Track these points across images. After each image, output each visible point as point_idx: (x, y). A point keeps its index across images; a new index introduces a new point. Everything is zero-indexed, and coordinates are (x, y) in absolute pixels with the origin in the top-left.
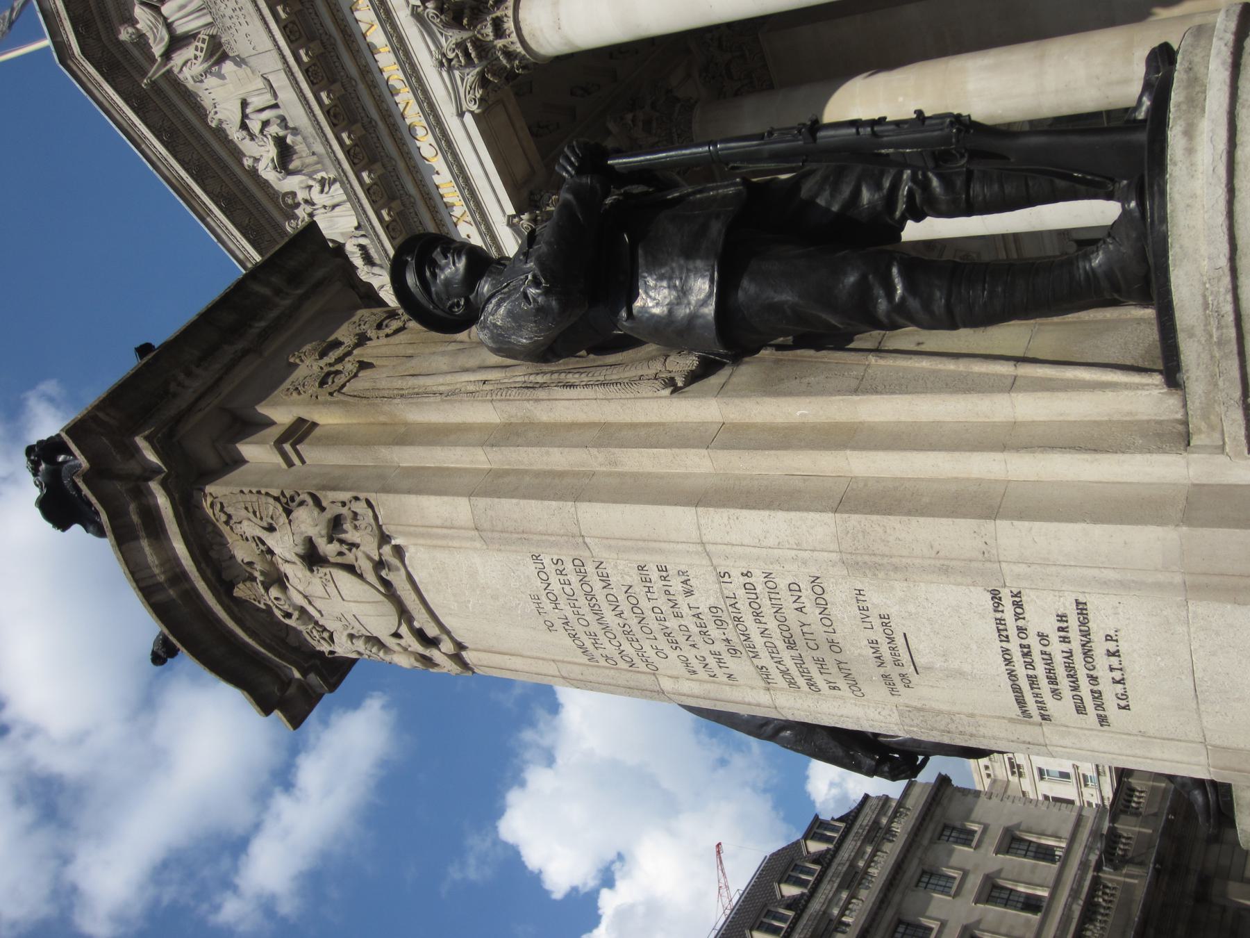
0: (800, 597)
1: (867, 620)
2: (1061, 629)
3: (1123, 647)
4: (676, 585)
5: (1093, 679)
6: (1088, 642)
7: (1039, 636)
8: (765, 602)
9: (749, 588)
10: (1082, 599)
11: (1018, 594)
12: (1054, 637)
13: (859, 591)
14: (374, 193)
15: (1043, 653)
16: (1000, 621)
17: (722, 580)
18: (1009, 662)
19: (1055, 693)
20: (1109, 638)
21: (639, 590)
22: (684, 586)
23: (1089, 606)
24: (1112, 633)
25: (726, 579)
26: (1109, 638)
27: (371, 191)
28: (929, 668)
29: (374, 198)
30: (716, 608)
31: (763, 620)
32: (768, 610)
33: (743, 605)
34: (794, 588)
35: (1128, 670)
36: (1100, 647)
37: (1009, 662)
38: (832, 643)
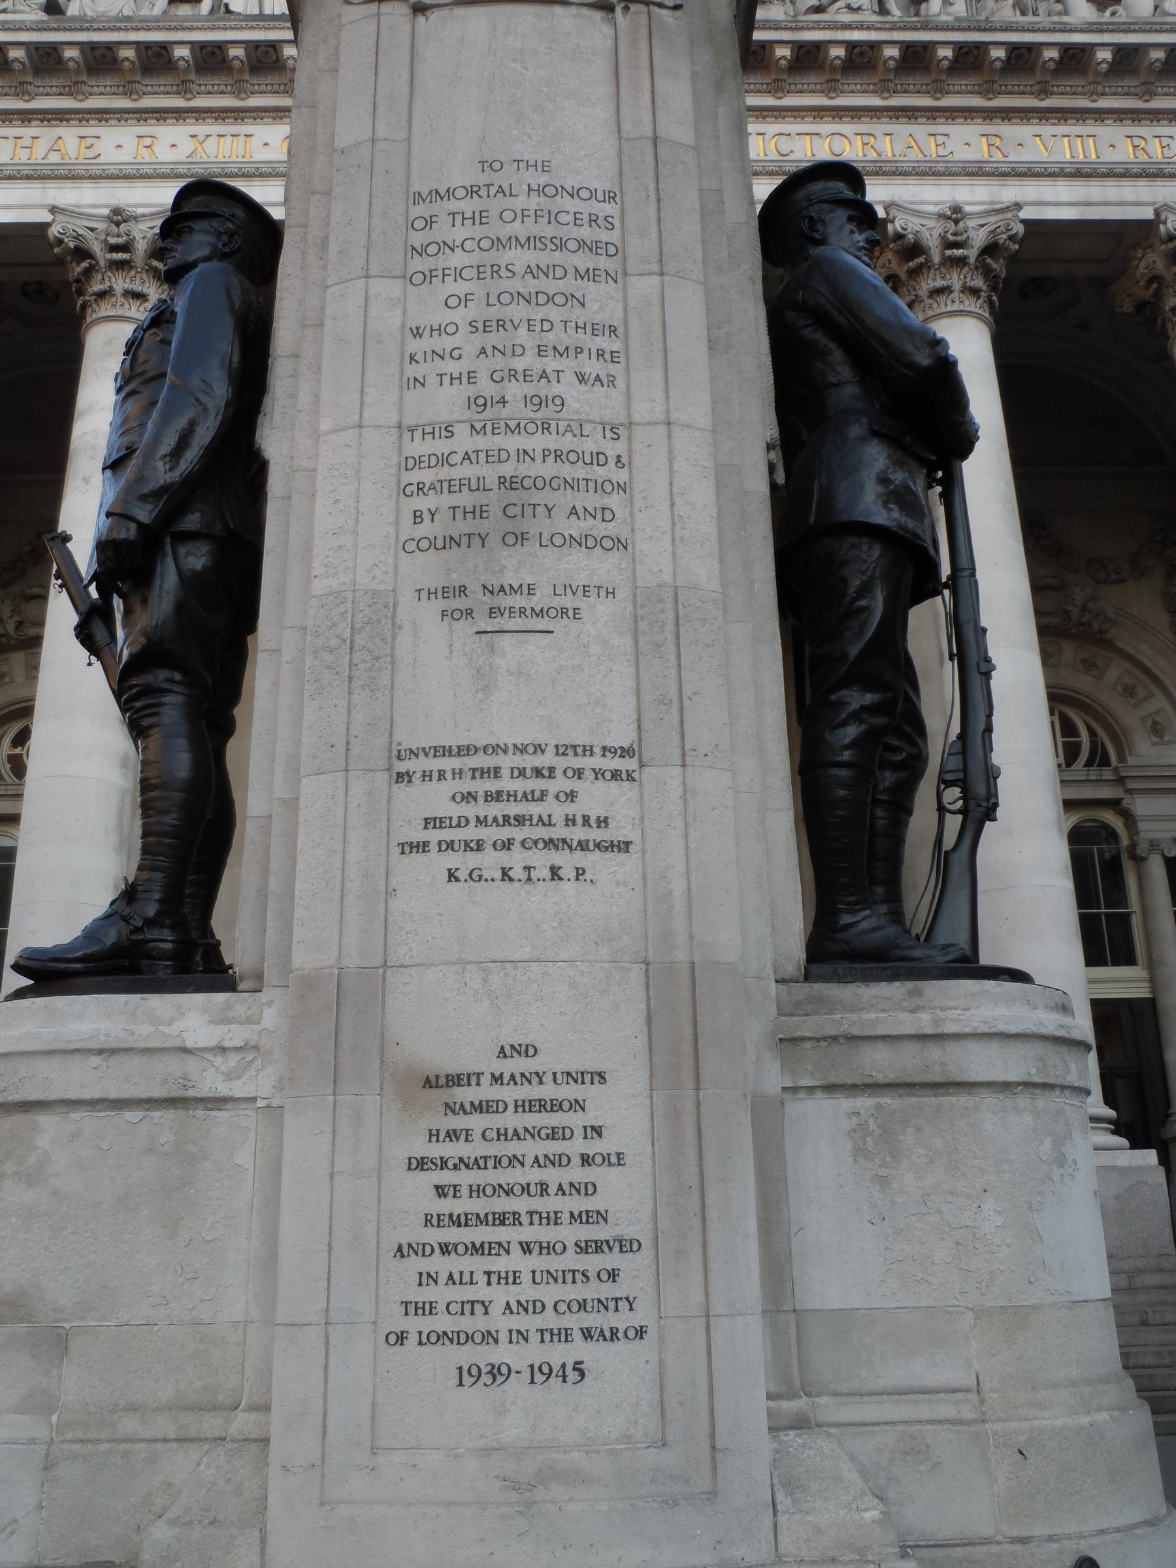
0: (594, 518)
1: (568, 590)
2: (586, 820)
3: (569, 888)
4: (592, 367)
5: (507, 845)
6: (570, 847)
7: (572, 792)
8: (581, 472)
9: (599, 458)
10: (632, 847)
11: (630, 777)
12: (570, 809)
13: (613, 593)
14: (267, 52)
15: (544, 793)
16: (588, 750)
17: (608, 428)
19: (469, 797)
20: (580, 872)
21: (578, 315)
22: (595, 375)
23: (624, 855)
24: (588, 876)
25: (609, 434)
26: (580, 872)
27: (271, 50)
28: (491, 648)
29: (261, 49)
30: (563, 404)
32: (565, 471)
33: (567, 442)
35: (528, 887)
36: (566, 860)
37: (521, 749)
38: (521, 538)
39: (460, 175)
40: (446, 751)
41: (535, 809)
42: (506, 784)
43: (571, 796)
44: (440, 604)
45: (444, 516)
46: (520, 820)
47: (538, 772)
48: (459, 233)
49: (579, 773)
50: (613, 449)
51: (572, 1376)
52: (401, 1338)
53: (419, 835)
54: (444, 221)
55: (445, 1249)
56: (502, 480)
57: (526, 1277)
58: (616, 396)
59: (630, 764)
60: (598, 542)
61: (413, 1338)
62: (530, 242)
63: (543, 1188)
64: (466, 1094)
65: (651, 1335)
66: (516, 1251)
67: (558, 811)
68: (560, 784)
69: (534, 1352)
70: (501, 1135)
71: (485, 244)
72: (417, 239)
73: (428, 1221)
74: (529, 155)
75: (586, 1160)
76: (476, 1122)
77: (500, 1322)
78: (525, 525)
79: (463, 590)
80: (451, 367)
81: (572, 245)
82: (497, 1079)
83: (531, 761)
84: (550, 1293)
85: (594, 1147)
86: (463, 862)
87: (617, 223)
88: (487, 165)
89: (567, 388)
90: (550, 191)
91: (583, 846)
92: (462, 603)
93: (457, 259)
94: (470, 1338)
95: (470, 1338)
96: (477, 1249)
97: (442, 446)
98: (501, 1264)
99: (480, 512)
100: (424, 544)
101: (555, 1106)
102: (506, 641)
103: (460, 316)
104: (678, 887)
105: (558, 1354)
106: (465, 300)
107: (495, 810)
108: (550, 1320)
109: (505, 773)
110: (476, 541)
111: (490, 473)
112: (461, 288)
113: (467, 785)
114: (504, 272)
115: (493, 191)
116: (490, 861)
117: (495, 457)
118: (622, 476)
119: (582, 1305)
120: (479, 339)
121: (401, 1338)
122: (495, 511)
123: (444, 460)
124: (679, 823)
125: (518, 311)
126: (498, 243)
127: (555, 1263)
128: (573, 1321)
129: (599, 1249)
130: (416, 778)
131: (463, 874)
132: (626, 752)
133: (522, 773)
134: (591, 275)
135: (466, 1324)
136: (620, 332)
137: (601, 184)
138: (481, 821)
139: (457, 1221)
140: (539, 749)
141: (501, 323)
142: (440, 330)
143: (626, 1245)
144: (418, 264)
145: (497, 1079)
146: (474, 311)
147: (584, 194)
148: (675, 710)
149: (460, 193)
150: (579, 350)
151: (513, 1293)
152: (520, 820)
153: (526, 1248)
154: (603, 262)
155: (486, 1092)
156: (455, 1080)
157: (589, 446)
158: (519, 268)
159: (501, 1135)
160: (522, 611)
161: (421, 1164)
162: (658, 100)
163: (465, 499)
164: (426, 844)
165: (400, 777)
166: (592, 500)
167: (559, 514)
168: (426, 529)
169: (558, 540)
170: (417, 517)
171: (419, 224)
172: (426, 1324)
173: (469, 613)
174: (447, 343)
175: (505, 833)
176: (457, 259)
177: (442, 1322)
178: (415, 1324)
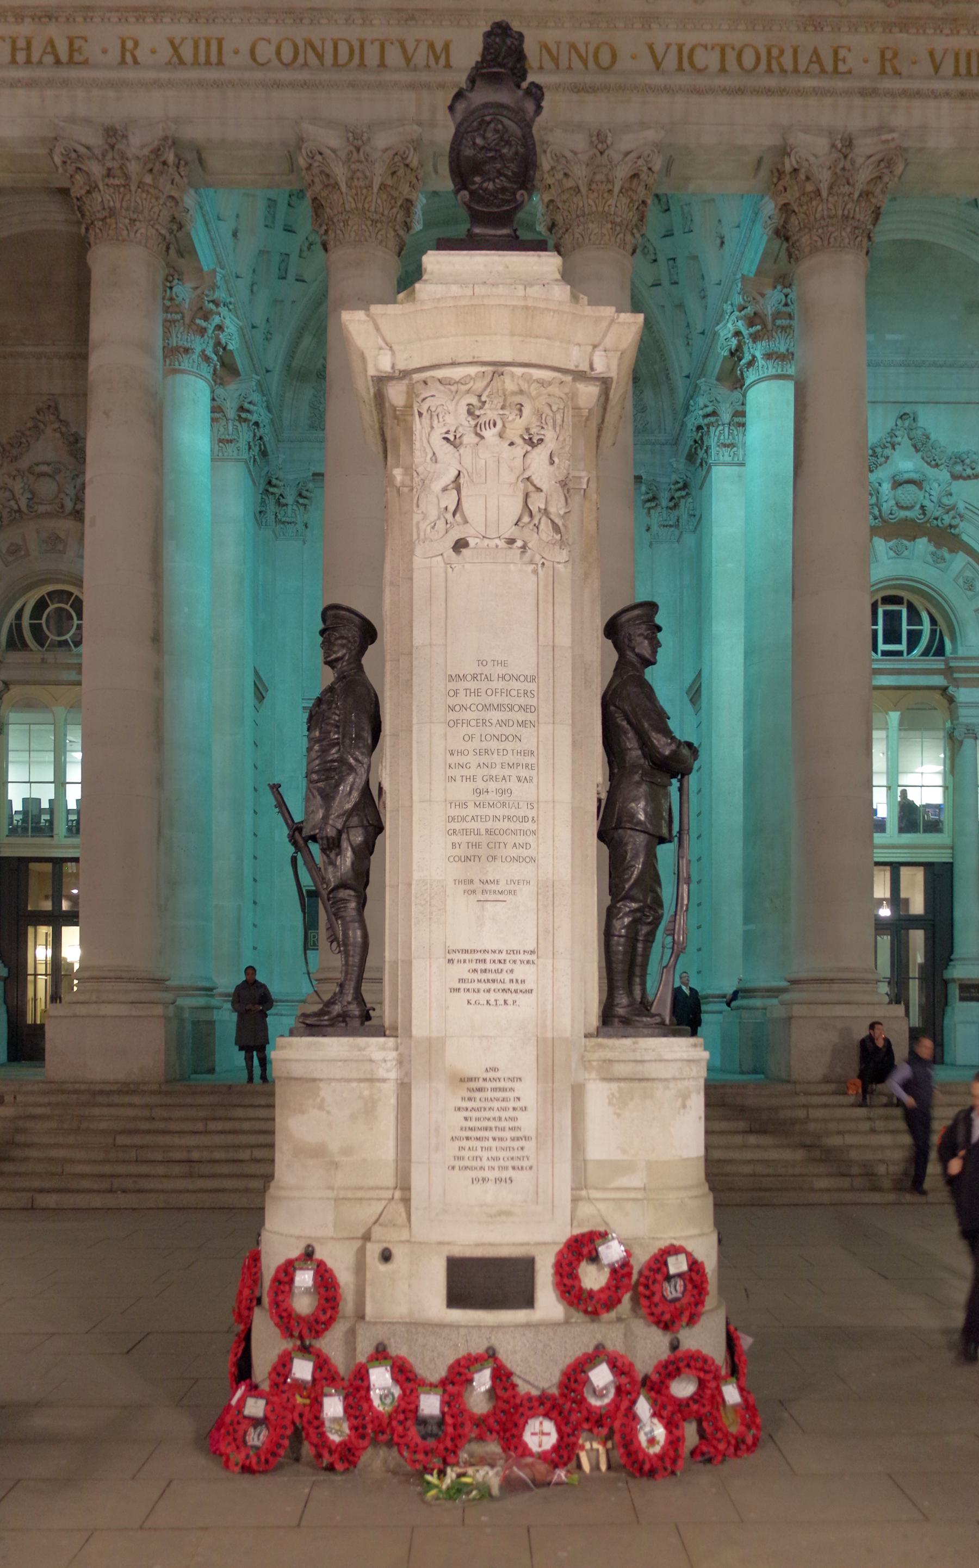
2: (517, 981)
3: (510, 1008)
4: (524, 773)
5: (489, 991)
9: (525, 819)
18: (494, 952)
19: (475, 971)
20: (514, 1002)
21: (518, 746)
26: (514, 1002)
28: (483, 908)
31: (506, 820)
33: (512, 812)
34: (526, 846)
37: (494, 952)
38: (494, 858)
39: (470, 668)
40: (467, 951)
41: (499, 977)
42: (489, 966)
43: (512, 971)
44: (462, 887)
45: (464, 846)
46: (494, 981)
47: (500, 962)
48: (468, 701)
49: (515, 962)
50: (531, 813)
51: (508, 1181)
52: (453, 1168)
53: (457, 985)
54: (462, 693)
55: (467, 1138)
56: (487, 831)
57: (494, 1149)
58: (533, 786)
59: (534, 957)
60: (524, 859)
61: (457, 1168)
62: (499, 707)
63: (500, 1119)
64: (473, 1085)
65: (535, 1168)
66: (491, 1139)
67: (507, 977)
68: (508, 966)
69: (497, 1174)
70: (487, 1099)
71: (480, 707)
72: (451, 701)
73: (461, 1129)
74: (499, 659)
75: (514, 1109)
76: (478, 1095)
77: (486, 1164)
78: (497, 852)
79: (472, 881)
80: (465, 772)
81: (516, 708)
82: (485, 1080)
83: (497, 957)
84: (502, 1154)
85: (518, 1104)
86: (472, 997)
87: (535, 694)
88: (481, 663)
89: (513, 785)
90: (507, 678)
91: (516, 991)
92: (471, 887)
93: (467, 715)
94: (476, 1168)
95: (476, 1168)
96: (478, 1139)
97: (463, 812)
98: (486, 1144)
99: (477, 845)
100: (457, 859)
101: (504, 1090)
102: (488, 905)
103: (471, 746)
104: (549, 1007)
105: (505, 1174)
106: (471, 738)
107: (484, 976)
108: (502, 1163)
109: (488, 961)
110: (477, 859)
111: (482, 826)
112: (471, 730)
113: (474, 966)
114: (488, 724)
115: (483, 676)
116: (483, 997)
117: (485, 819)
118: (533, 827)
119: (512, 1159)
120: (478, 759)
121: (453, 1168)
122: (484, 845)
123: (464, 819)
124: (550, 982)
125: (494, 745)
126: (486, 707)
127: (503, 1144)
128: (509, 1164)
129: (518, 1139)
130: (455, 961)
131: (473, 1002)
132: (532, 952)
133: (494, 961)
134: (522, 724)
135: (474, 1164)
136: (535, 754)
137: (530, 672)
138: (479, 981)
139: (471, 1129)
140: (500, 952)
141: (486, 752)
142: (462, 753)
143: (527, 1138)
144: (453, 716)
145: (485, 1080)
146: (475, 744)
147: (522, 678)
148: (551, 935)
149: (469, 678)
150: (518, 765)
151: (490, 1154)
152: (494, 981)
153: (494, 1139)
154: (531, 717)
155: (481, 1084)
156: (470, 1080)
157: (521, 813)
158: (494, 722)
159: (487, 1099)
160: (495, 892)
161: (459, 1109)
162: (556, 622)
163: (472, 838)
164: (459, 990)
165: (449, 961)
166: (520, 839)
167: (509, 846)
168: (457, 852)
169: (509, 859)
170: (453, 845)
171: (452, 693)
172: (462, 1163)
173: (474, 892)
174: (463, 760)
175: (488, 986)
176: (467, 715)
177: (466, 1163)
178: (457, 1163)
